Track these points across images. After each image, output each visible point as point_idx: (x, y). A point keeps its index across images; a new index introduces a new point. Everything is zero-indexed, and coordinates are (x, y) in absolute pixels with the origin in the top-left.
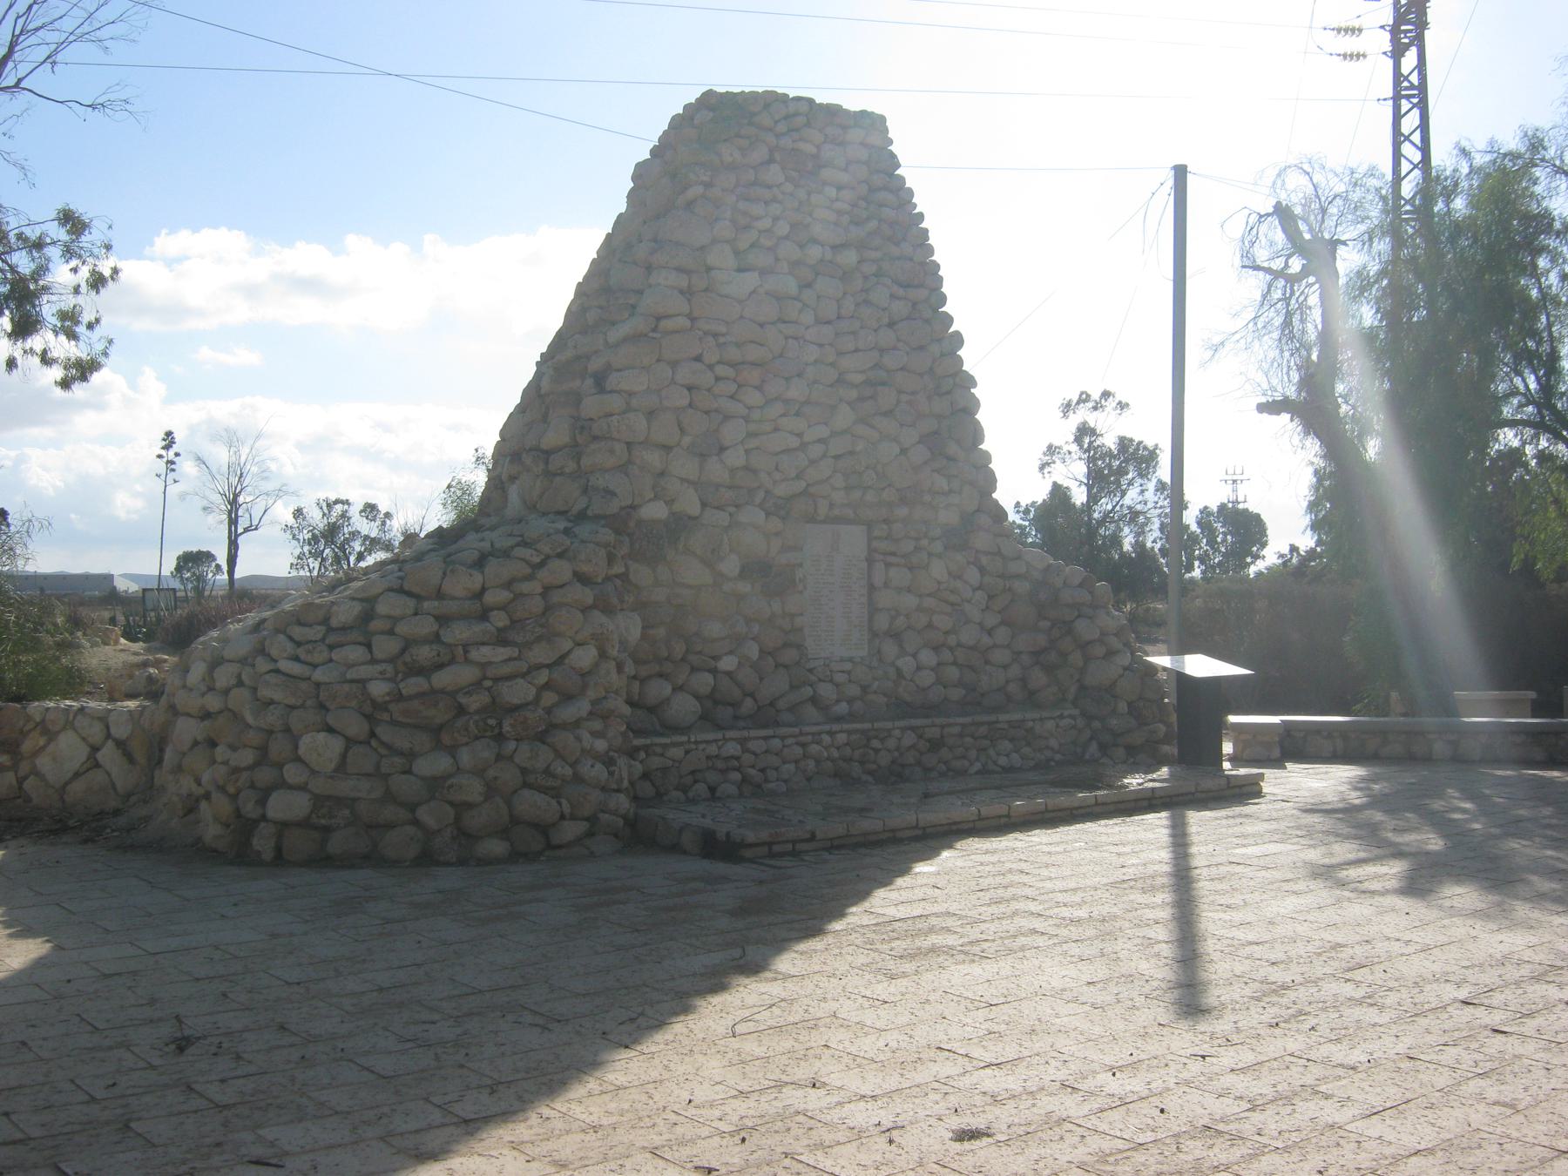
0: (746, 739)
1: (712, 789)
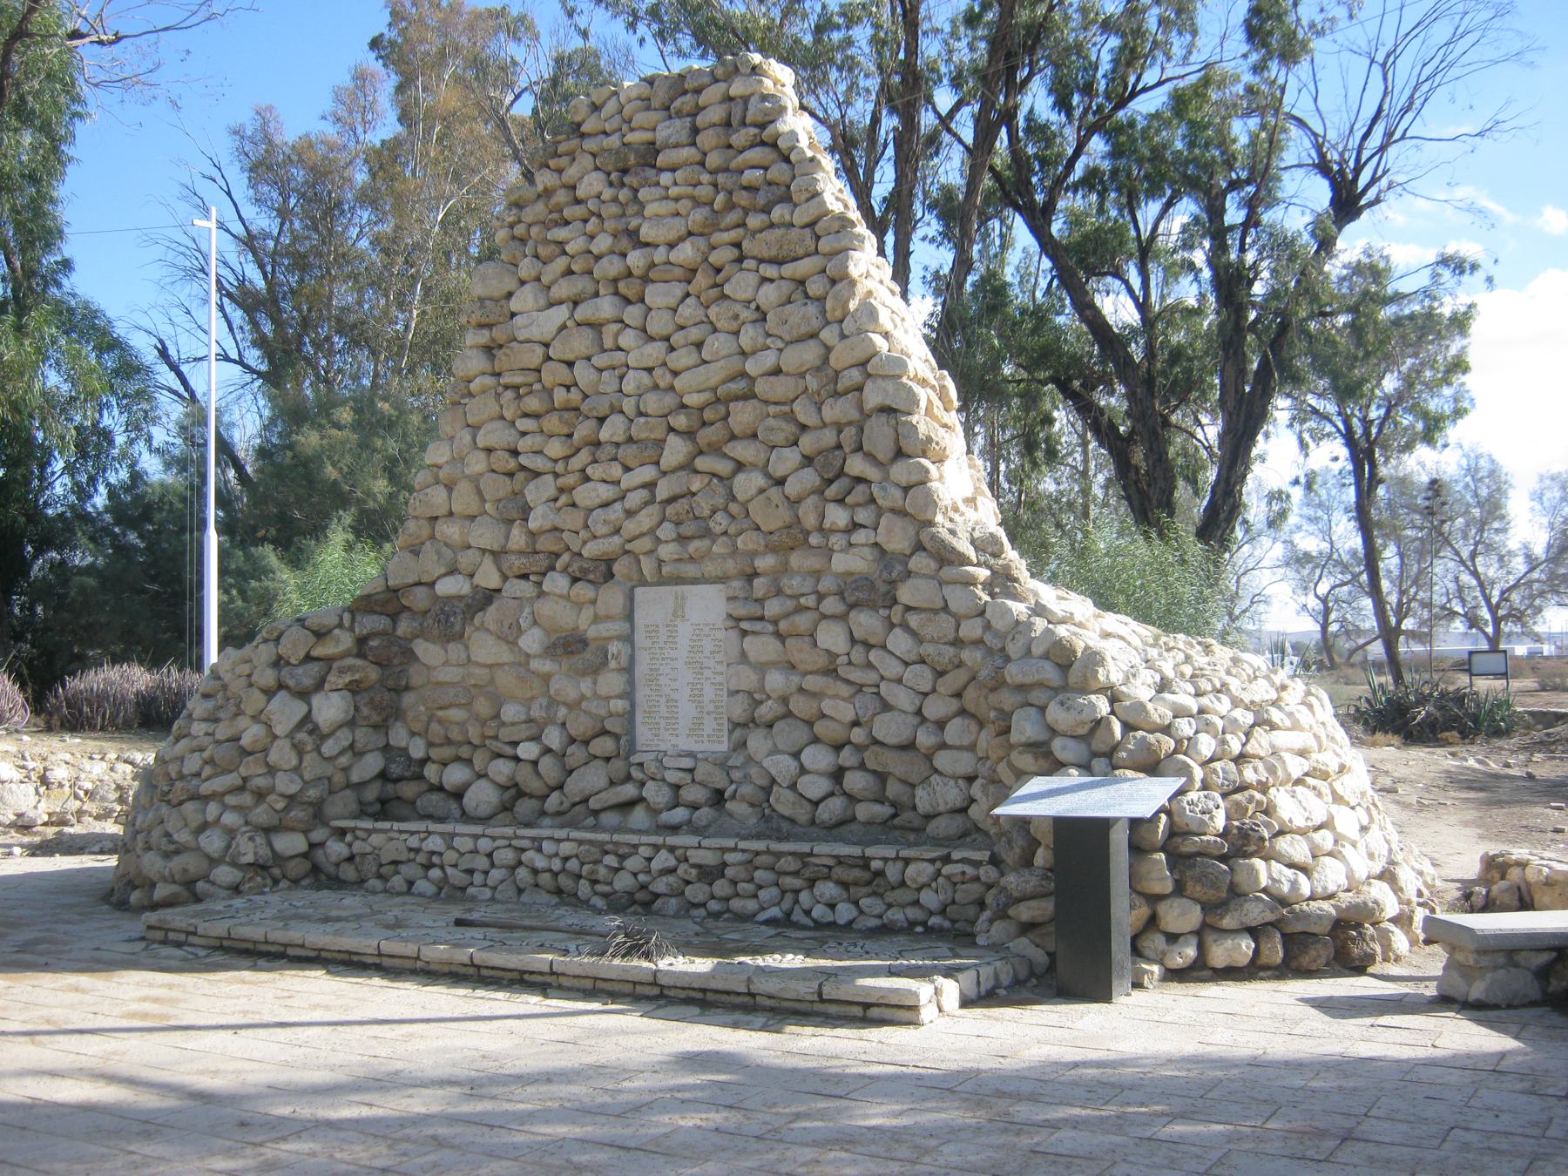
0: (453, 835)
1: (411, 883)
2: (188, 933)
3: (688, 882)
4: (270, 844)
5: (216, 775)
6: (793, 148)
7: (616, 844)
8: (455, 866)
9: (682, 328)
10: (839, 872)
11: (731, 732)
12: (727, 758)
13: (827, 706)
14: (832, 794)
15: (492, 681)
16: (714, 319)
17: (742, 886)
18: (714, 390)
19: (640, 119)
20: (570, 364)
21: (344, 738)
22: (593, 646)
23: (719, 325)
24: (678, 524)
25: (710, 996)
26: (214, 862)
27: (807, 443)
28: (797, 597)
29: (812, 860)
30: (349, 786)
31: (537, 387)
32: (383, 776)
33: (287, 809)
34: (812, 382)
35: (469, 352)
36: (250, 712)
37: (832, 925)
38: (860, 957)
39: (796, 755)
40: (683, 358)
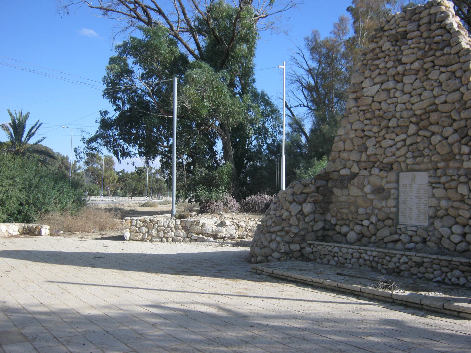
0: (341, 247)
1: (329, 261)
2: (262, 271)
3: (412, 267)
4: (289, 247)
5: (276, 226)
6: (451, 28)
7: (390, 253)
8: (342, 257)
9: (415, 89)
10: (461, 267)
11: (429, 219)
12: (428, 228)
13: (461, 212)
14: (461, 241)
15: (356, 201)
16: (425, 86)
17: (429, 269)
18: (425, 109)
19: (402, 24)
20: (380, 103)
21: (312, 216)
22: (386, 191)
23: (427, 88)
24: (413, 152)
25: (408, 304)
26: (273, 251)
27: (455, 125)
28: (451, 176)
29: (452, 262)
30: (313, 231)
31: (370, 110)
32: (324, 228)
33: (294, 237)
34: (457, 105)
35: (350, 100)
36: (285, 208)
37: (458, 285)
38: (463, 296)
39: (450, 228)
40: (415, 99)
